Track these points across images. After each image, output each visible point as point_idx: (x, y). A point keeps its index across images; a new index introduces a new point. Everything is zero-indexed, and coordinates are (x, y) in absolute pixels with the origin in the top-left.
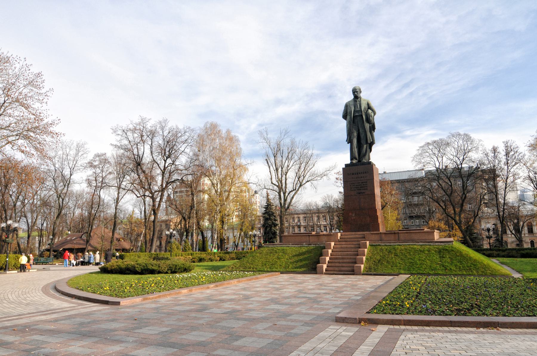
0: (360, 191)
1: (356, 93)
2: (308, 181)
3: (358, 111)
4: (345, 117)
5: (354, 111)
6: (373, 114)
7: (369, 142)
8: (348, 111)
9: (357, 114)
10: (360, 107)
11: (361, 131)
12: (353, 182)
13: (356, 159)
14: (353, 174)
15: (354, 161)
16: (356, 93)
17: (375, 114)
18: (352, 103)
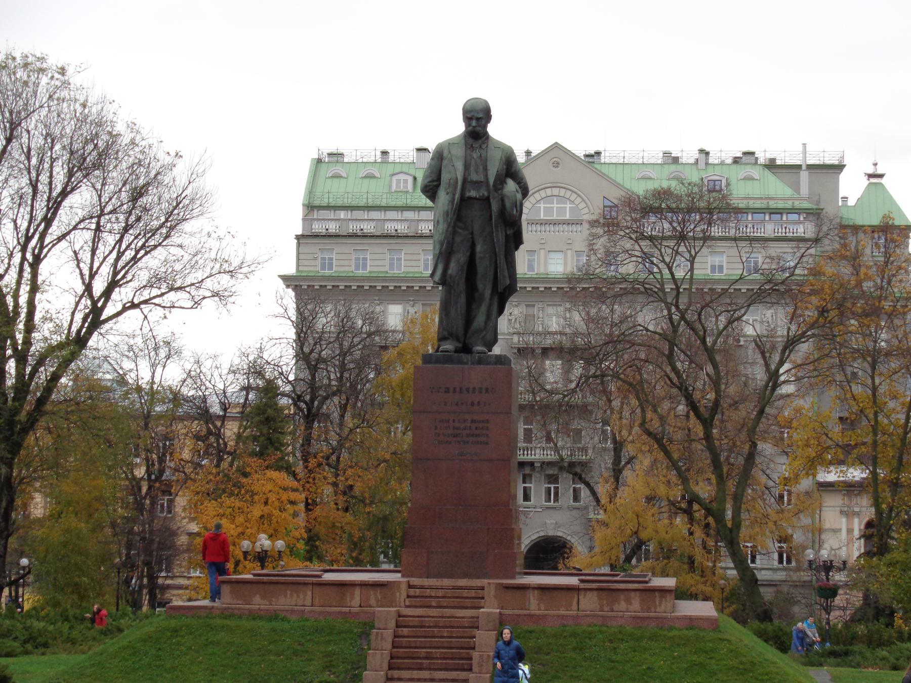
1: (477, 117)
2: (134, 306)
3: (477, 184)
4: (431, 190)
5: (465, 181)
6: (519, 196)
7: (500, 288)
8: (445, 177)
9: (473, 194)
10: (486, 169)
11: (478, 248)
13: (458, 340)
14: (447, 391)
15: (448, 346)
16: (477, 117)
17: (525, 192)
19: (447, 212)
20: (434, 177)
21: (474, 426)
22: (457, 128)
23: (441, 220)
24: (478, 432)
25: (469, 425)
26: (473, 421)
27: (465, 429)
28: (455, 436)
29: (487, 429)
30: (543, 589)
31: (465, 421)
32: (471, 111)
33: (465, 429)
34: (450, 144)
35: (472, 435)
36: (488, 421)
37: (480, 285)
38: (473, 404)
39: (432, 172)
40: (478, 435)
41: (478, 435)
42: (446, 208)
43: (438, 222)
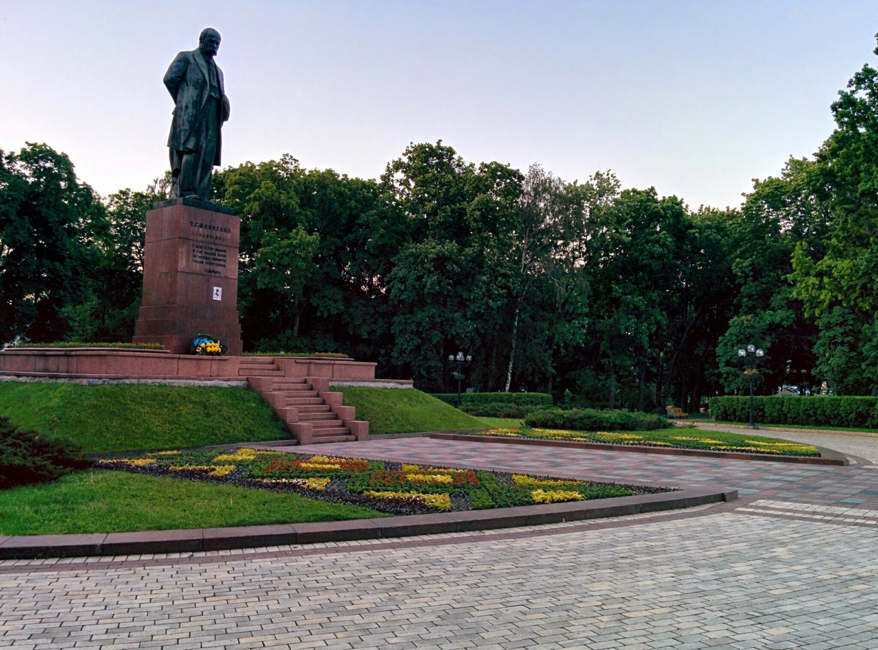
0: (212, 268)
1: (210, 42)
9: (213, 94)
11: (210, 132)
12: (200, 244)
14: (201, 226)
16: (210, 42)
18: (201, 61)
19: (196, 101)
20: (180, 74)
21: (217, 253)
22: (193, 45)
23: (190, 106)
24: (221, 258)
25: (213, 252)
26: (217, 250)
27: (212, 254)
28: (206, 258)
29: (225, 256)
30: (316, 364)
31: (212, 249)
32: (211, 36)
33: (212, 254)
34: (193, 53)
35: (216, 259)
36: (225, 251)
37: (207, 159)
38: (216, 238)
39: (179, 70)
40: (220, 260)
41: (220, 260)
42: (195, 98)
43: (187, 107)
